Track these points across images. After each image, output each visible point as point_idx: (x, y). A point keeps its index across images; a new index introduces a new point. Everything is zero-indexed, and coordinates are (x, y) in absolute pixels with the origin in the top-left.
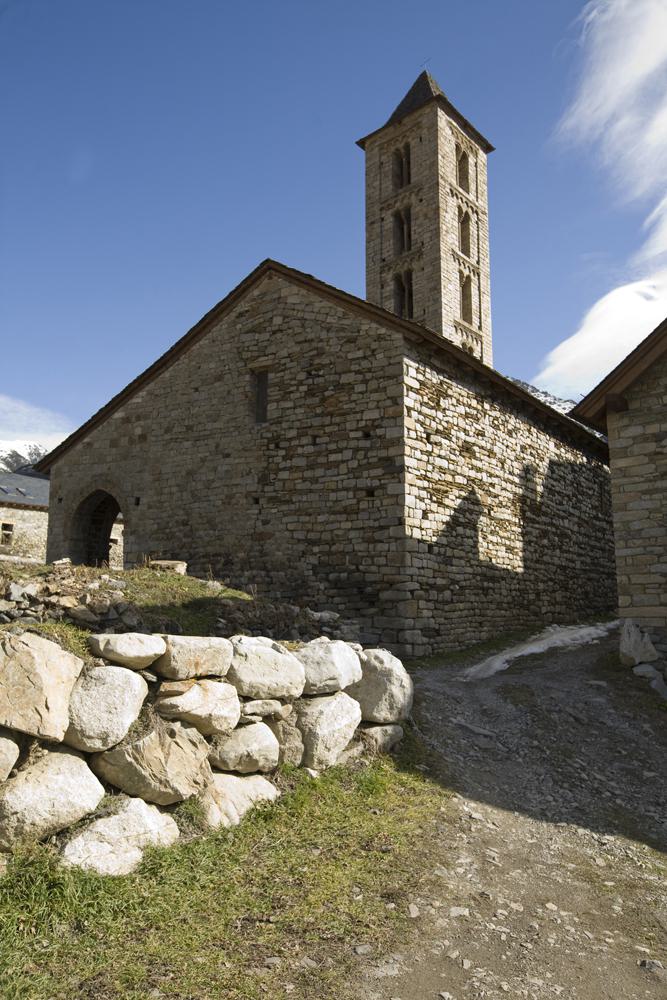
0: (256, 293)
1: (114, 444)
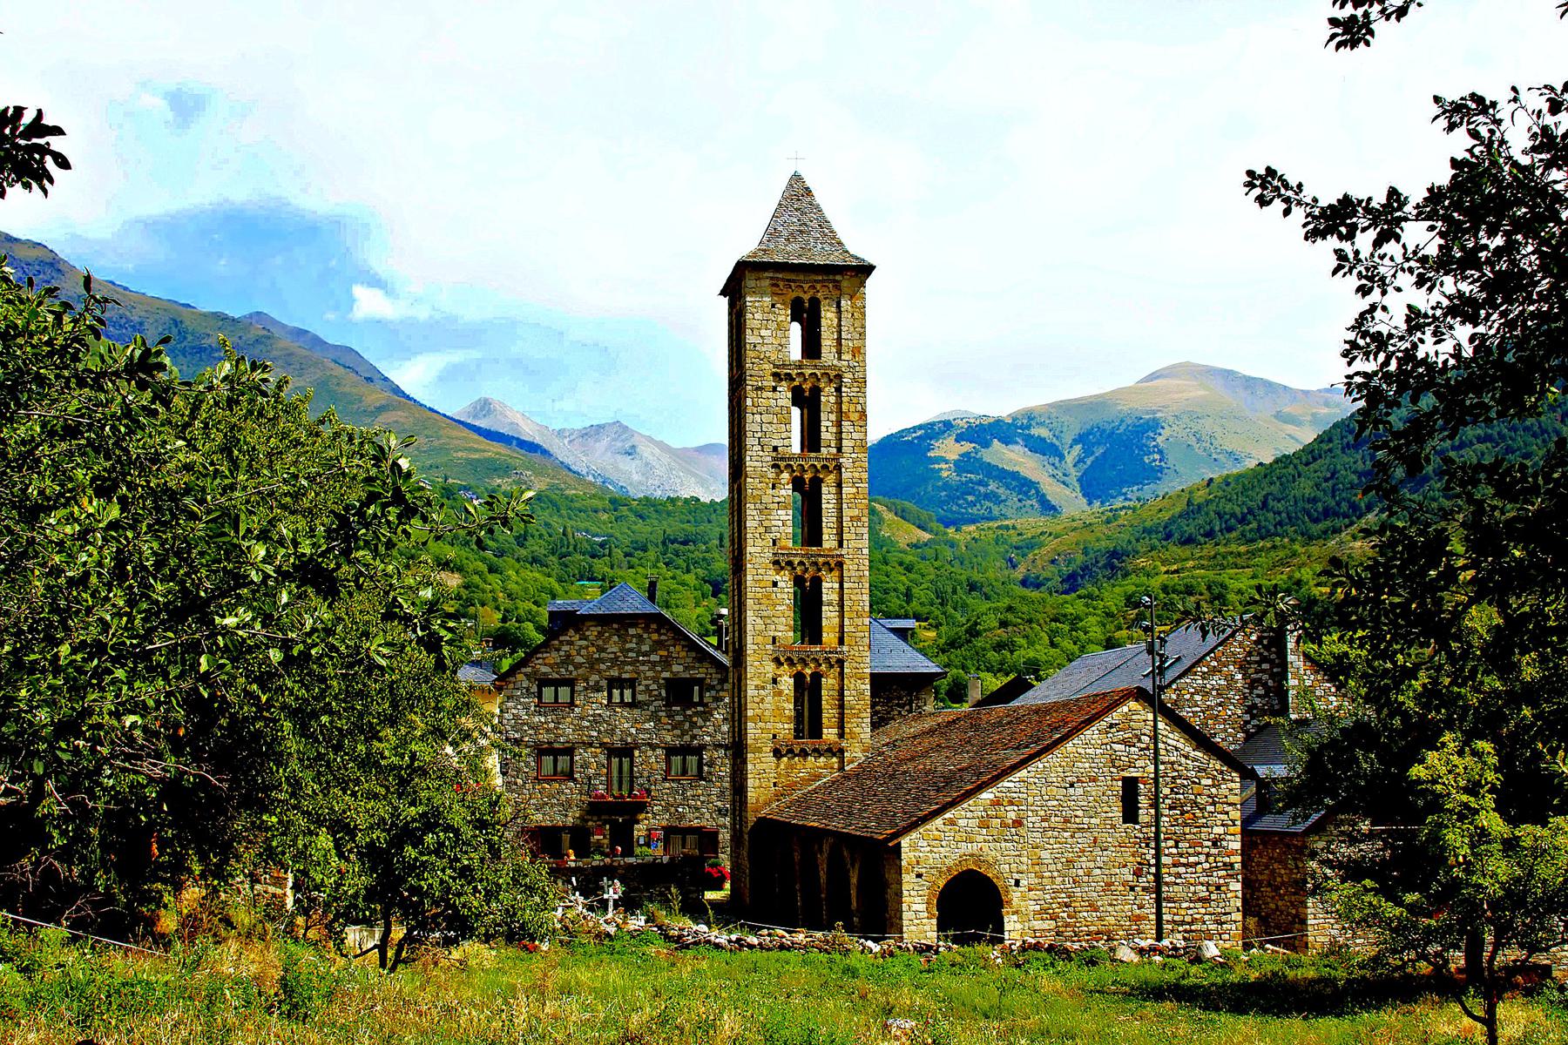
0: (1125, 709)
1: (984, 824)
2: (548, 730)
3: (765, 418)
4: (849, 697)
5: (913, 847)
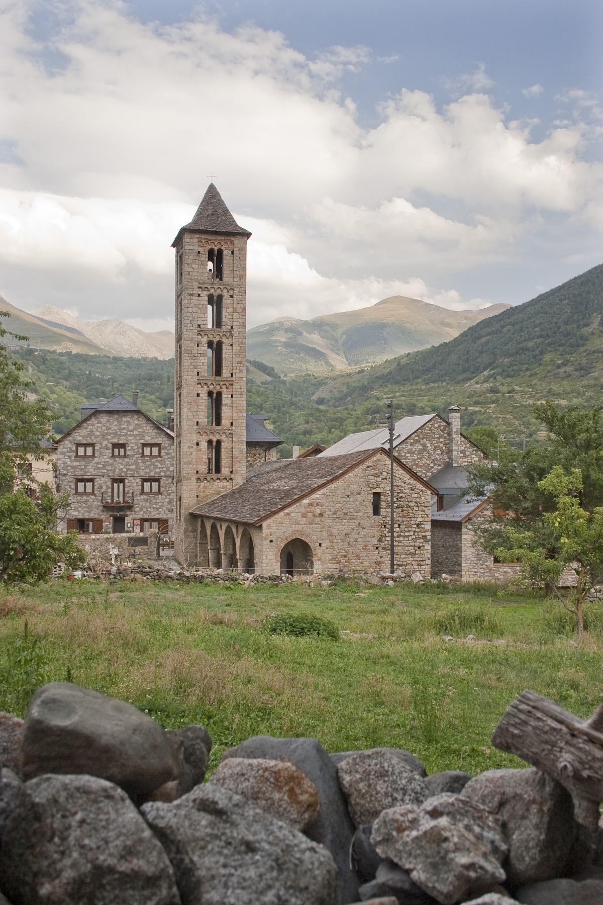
0: (375, 459)
1: (304, 516)
2: (81, 470)
3: (195, 310)
4: (236, 453)
5: (269, 527)
